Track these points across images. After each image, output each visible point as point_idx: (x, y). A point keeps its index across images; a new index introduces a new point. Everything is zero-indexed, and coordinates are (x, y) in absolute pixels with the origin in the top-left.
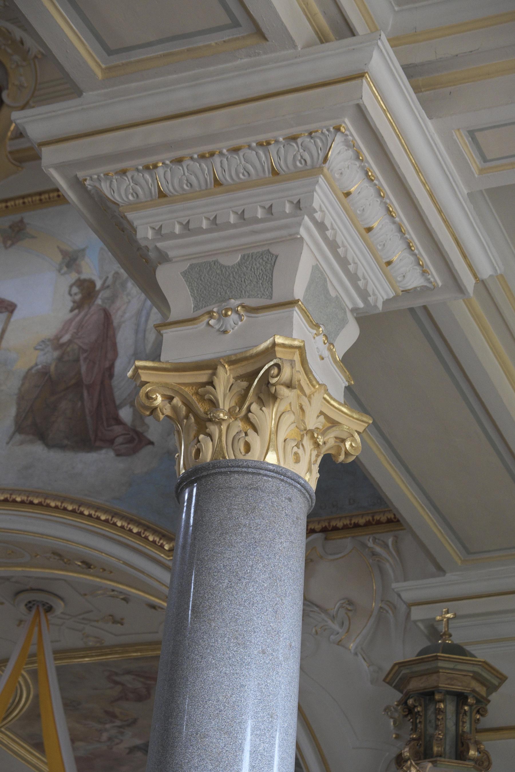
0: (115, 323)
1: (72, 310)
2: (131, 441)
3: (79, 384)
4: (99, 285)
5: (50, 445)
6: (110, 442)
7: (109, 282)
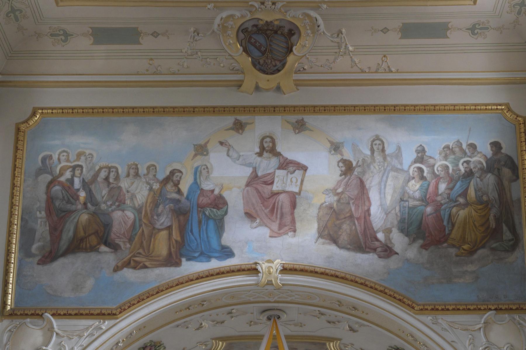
0: (367, 186)
1: (341, 175)
2: (386, 251)
3: (351, 217)
4: (354, 164)
6: (374, 250)
7: (360, 163)
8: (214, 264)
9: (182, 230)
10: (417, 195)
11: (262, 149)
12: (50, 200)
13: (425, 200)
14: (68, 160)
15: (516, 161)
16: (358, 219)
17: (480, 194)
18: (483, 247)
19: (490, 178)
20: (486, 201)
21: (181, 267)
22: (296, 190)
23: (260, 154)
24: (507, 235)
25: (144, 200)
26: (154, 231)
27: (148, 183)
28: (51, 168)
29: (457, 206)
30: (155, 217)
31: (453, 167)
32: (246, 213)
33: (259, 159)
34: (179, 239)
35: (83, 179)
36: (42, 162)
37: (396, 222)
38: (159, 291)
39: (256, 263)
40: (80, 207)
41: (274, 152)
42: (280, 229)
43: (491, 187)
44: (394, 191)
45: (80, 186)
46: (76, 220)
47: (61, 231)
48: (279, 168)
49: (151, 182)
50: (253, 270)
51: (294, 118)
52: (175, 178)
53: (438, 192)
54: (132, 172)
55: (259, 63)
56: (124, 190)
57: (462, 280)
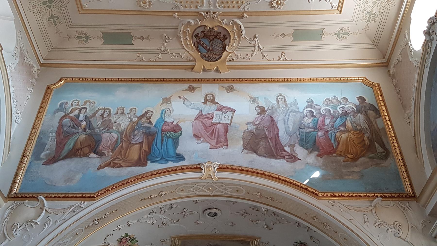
1: (257, 115)
2: (292, 158)
4: (266, 109)
5: (259, 155)
6: (284, 157)
8: (170, 165)
9: (150, 145)
10: (310, 125)
11: (206, 100)
12: (61, 126)
13: (316, 128)
14: (78, 105)
15: (377, 107)
16: (270, 139)
17: (355, 125)
18: (363, 156)
19: (360, 117)
20: (360, 129)
21: (147, 167)
22: (229, 122)
23: (205, 103)
24: (379, 149)
25: (126, 127)
26: (130, 145)
27: (129, 118)
28: (65, 109)
29: (339, 132)
30: (132, 137)
31: (333, 110)
32: (194, 135)
33: (204, 105)
34: (147, 149)
35: (86, 115)
36: (60, 106)
37: (297, 141)
38: (128, 182)
39: (200, 164)
40: (81, 130)
41: (213, 101)
42: (217, 144)
43: (362, 122)
44: (294, 123)
45: (83, 119)
46: (76, 138)
47: (65, 145)
48: (216, 111)
49: (132, 117)
50: (198, 168)
51: (227, 85)
52: (148, 115)
53: (325, 124)
54: (120, 112)
55: (205, 56)
56: (113, 122)
57: (351, 177)
